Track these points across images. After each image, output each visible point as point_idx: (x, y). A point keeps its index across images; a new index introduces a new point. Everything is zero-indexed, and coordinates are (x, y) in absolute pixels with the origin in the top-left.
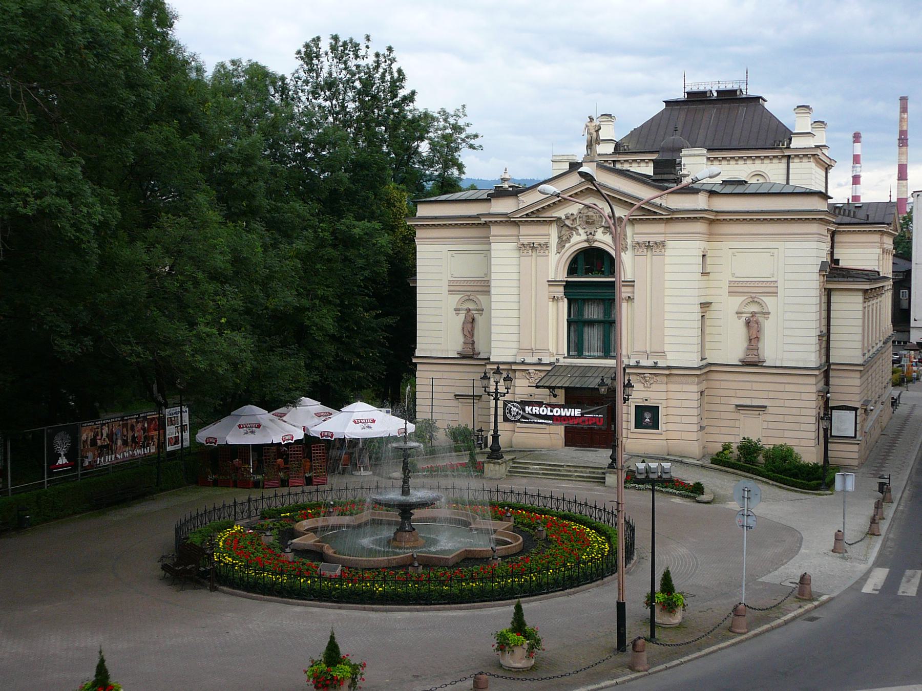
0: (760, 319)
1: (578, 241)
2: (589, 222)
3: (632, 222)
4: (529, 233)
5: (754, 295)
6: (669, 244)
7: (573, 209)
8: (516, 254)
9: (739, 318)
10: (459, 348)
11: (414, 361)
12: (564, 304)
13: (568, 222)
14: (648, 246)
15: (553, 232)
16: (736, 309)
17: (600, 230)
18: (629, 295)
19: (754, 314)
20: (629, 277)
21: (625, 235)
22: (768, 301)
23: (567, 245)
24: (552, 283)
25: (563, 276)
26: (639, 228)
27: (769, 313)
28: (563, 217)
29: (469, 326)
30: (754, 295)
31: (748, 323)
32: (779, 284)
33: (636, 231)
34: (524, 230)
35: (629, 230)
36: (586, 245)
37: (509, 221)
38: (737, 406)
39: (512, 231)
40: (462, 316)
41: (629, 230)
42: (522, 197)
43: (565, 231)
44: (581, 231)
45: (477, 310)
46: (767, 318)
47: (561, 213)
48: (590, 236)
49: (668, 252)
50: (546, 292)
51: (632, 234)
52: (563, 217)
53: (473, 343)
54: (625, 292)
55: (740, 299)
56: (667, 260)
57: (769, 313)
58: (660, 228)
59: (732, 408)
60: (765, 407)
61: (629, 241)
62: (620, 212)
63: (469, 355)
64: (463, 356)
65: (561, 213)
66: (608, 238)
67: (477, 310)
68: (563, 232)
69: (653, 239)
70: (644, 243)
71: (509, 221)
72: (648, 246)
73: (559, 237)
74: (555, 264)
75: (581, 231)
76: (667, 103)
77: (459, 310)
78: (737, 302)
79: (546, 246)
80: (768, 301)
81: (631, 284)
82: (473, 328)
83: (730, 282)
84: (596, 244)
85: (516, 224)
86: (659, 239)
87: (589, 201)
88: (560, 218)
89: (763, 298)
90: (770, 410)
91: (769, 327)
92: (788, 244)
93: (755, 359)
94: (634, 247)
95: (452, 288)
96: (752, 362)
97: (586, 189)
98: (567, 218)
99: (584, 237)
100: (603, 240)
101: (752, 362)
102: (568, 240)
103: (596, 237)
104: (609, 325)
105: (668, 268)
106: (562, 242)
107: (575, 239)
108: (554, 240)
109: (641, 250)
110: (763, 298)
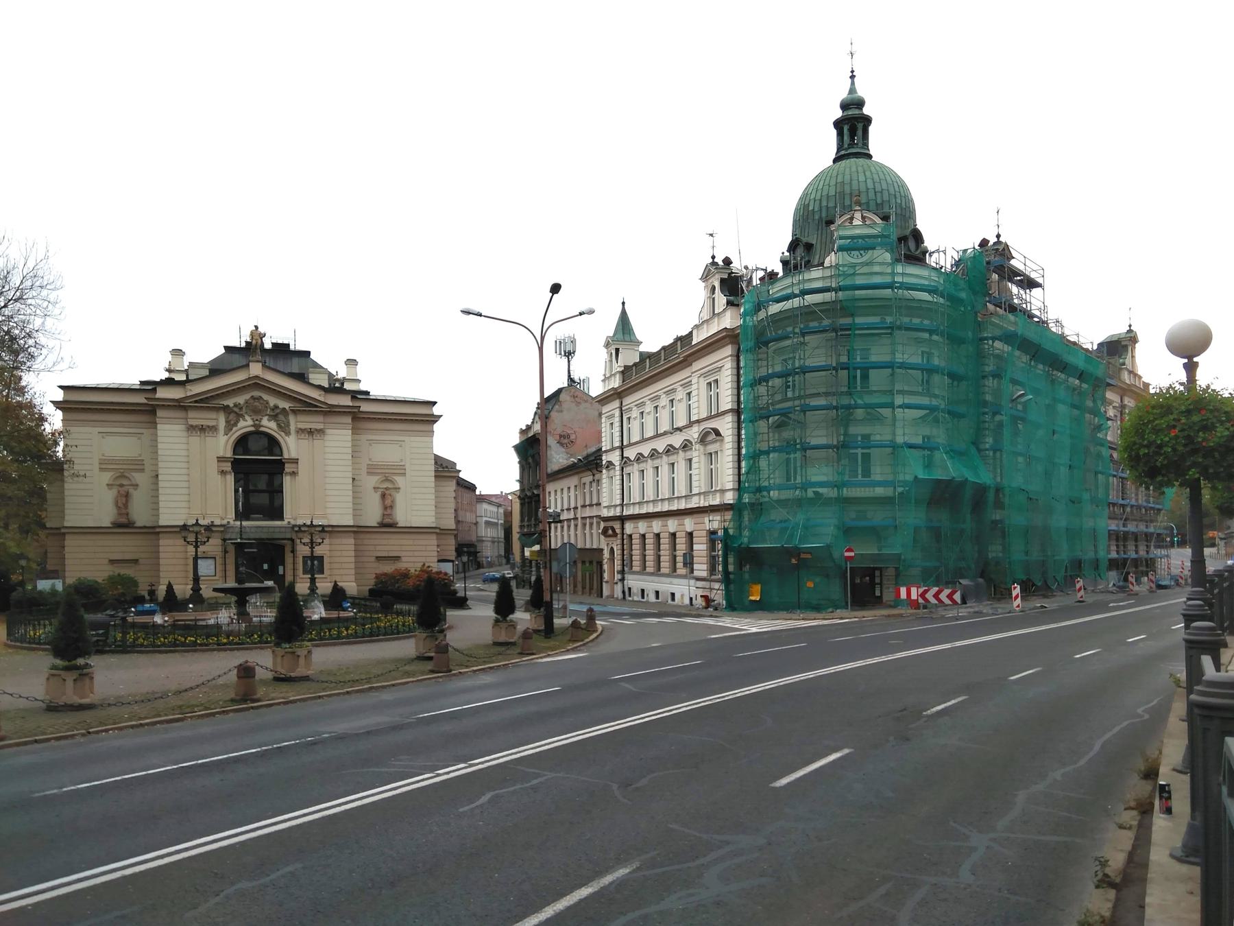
0: (393, 492)
1: (245, 425)
3: (294, 412)
4: (197, 418)
6: (328, 431)
7: (241, 399)
8: (185, 434)
12: (230, 479)
14: (311, 432)
15: (222, 421)
20: (294, 455)
22: (400, 481)
24: (221, 459)
25: (229, 454)
26: (301, 418)
31: (383, 496)
34: (191, 414)
35: (292, 419)
36: (252, 429)
37: (179, 405)
39: (180, 414)
41: (292, 419)
42: (188, 387)
43: (232, 416)
44: (247, 417)
47: (230, 402)
49: (327, 437)
50: (213, 467)
51: (294, 422)
54: (288, 468)
58: (321, 418)
61: (293, 428)
65: (230, 402)
66: (273, 425)
69: (313, 426)
71: (179, 405)
72: (311, 432)
73: (227, 422)
74: (222, 444)
75: (247, 417)
76: (225, 347)
78: (373, 481)
79: (214, 429)
80: (397, 478)
81: (296, 461)
82: (127, 501)
84: (262, 429)
85: (185, 408)
86: (320, 426)
87: (256, 393)
91: (400, 499)
92: (413, 439)
98: (235, 405)
99: (250, 422)
100: (269, 425)
102: (235, 424)
106: (230, 426)
107: (242, 424)
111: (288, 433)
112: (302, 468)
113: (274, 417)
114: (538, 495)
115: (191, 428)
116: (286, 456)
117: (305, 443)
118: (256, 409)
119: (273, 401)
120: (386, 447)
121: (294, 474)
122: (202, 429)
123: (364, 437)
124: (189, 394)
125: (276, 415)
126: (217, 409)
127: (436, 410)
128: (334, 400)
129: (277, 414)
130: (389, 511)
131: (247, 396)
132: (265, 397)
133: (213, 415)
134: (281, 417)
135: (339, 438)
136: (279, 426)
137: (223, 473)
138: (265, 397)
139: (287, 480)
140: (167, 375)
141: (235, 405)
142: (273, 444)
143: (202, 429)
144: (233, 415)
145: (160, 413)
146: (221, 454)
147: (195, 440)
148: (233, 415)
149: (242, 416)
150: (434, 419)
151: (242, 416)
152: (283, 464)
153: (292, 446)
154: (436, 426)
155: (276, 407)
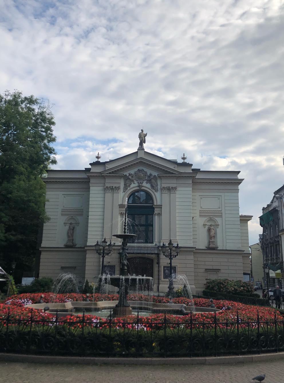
1: (134, 186)
2: (139, 178)
3: (160, 177)
4: (109, 183)
5: (211, 217)
6: (178, 189)
7: (132, 172)
8: (102, 192)
9: (205, 227)
10: (65, 242)
11: (40, 249)
13: (130, 177)
14: (169, 189)
15: (121, 183)
16: (203, 224)
17: (145, 182)
18: (159, 212)
19: (211, 225)
20: (159, 203)
21: (157, 184)
22: (219, 220)
23: (129, 188)
24: (121, 206)
26: (164, 181)
27: (219, 225)
28: (128, 175)
29: (72, 231)
30: (211, 217)
31: (209, 230)
32: (223, 212)
33: (163, 182)
34: (107, 180)
35: (159, 182)
36: (138, 188)
37: (101, 176)
38: (206, 269)
40: (67, 227)
44: (135, 182)
45: (76, 223)
46: (218, 227)
47: (127, 173)
48: (141, 184)
49: (177, 192)
50: (117, 211)
52: (128, 175)
53: (73, 240)
54: (156, 211)
55: (205, 219)
56: (177, 196)
57: (219, 225)
58: (175, 181)
59: (203, 270)
60: (220, 269)
61: (159, 187)
62: (155, 173)
63: (70, 246)
64: (67, 246)
66: (148, 186)
67: (76, 223)
68: (127, 182)
69: (171, 186)
70: (167, 187)
71: (101, 176)
73: (125, 185)
74: (122, 198)
75: (135, 182)
77: (66, 223)
79: (118, 188)
83: (200, 211)
84: (143, 188)
87: (141, 168)
88: (126, 175)
89: (216, 218)
90: (222, 271)
91: (219, 230)
93: (214, 246)
94: (161, 189)
95: (63, 213)
96: (212, 248)
97: (139, 162)
98: (130, 175)
99: (137, 185)
100: (146, 186)
101: (212, 248)
103: (143, 185)
104: (149, 227)
105: (177, 200)
106: (126, 187)
107: (133, 185)
108: (122, 186)
109: (165, 191)
110: (216, 218)
111: (157, 191)
112: (165, 211)
113: (149, 181)
114: (278, 241)
115: (106, 189)
116: (155, 204)
117: (166, 196)
118: (139, 176)
119: (149, 172)
120: (208, 201)
121: (160, 214)
122: (112, 189)
123: (198, 194)
124: (107, 169)
125: (150, 180)
126: (120, 177)
127: (240, 176)
128: (182, 170)
129: (150, 179)
130: (213, 240)
131: (136, 170)
132: (145, 170)
133: (118, 181)
134: (153, 181)
135: (184, 193)
136: (152, 186)
137: (122, 214)
138: (145, 170)
139: (156, 218)
140: (97, 160)
141: (130, 175)
142: (149, 197)
143: (112, 189)
144: (128, 180)
145: (92, 181)
146: (120, 203)
147: (109, 195)
148: (128, 180)
149: (133, 181)
150: (240, 181)
151: (133, 181)
152: (154, 208)
153: (158, 198)
154: (240, 187)
155: (151, 175)
